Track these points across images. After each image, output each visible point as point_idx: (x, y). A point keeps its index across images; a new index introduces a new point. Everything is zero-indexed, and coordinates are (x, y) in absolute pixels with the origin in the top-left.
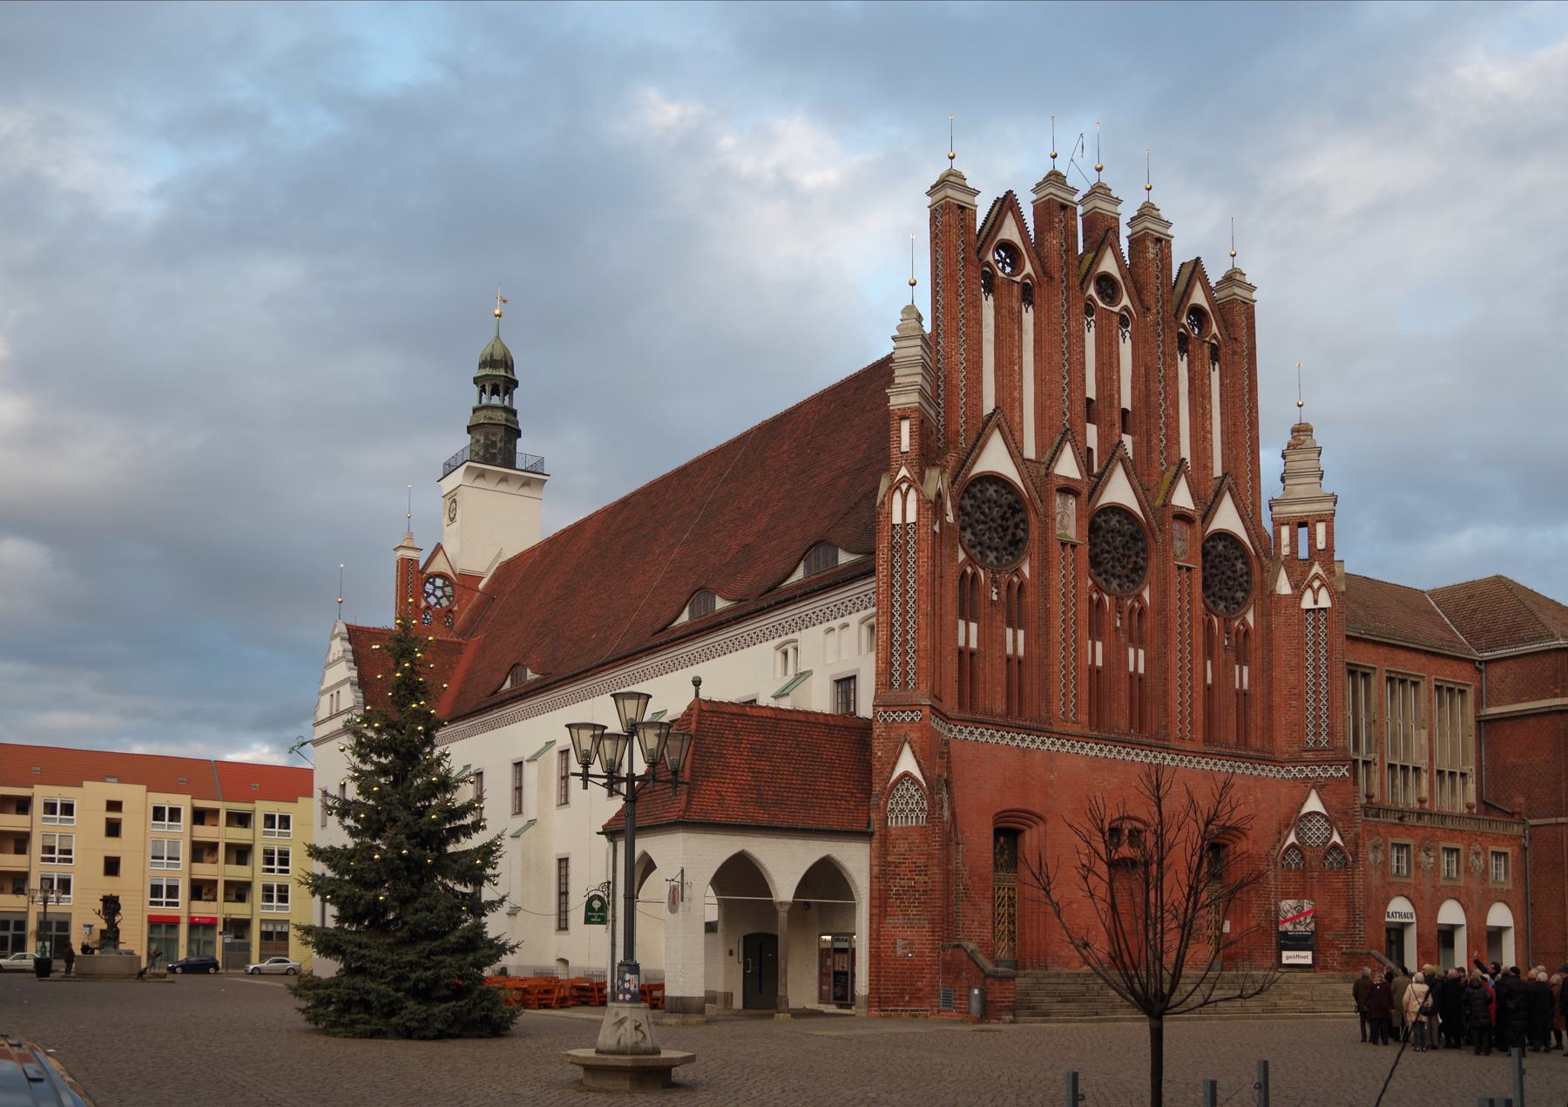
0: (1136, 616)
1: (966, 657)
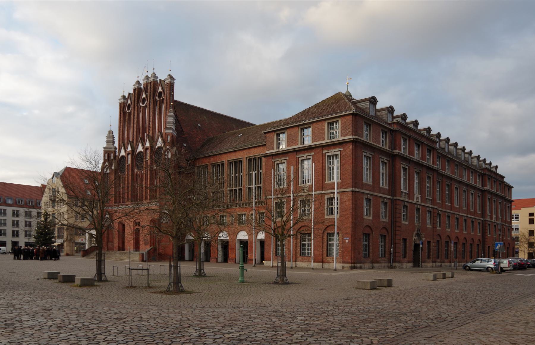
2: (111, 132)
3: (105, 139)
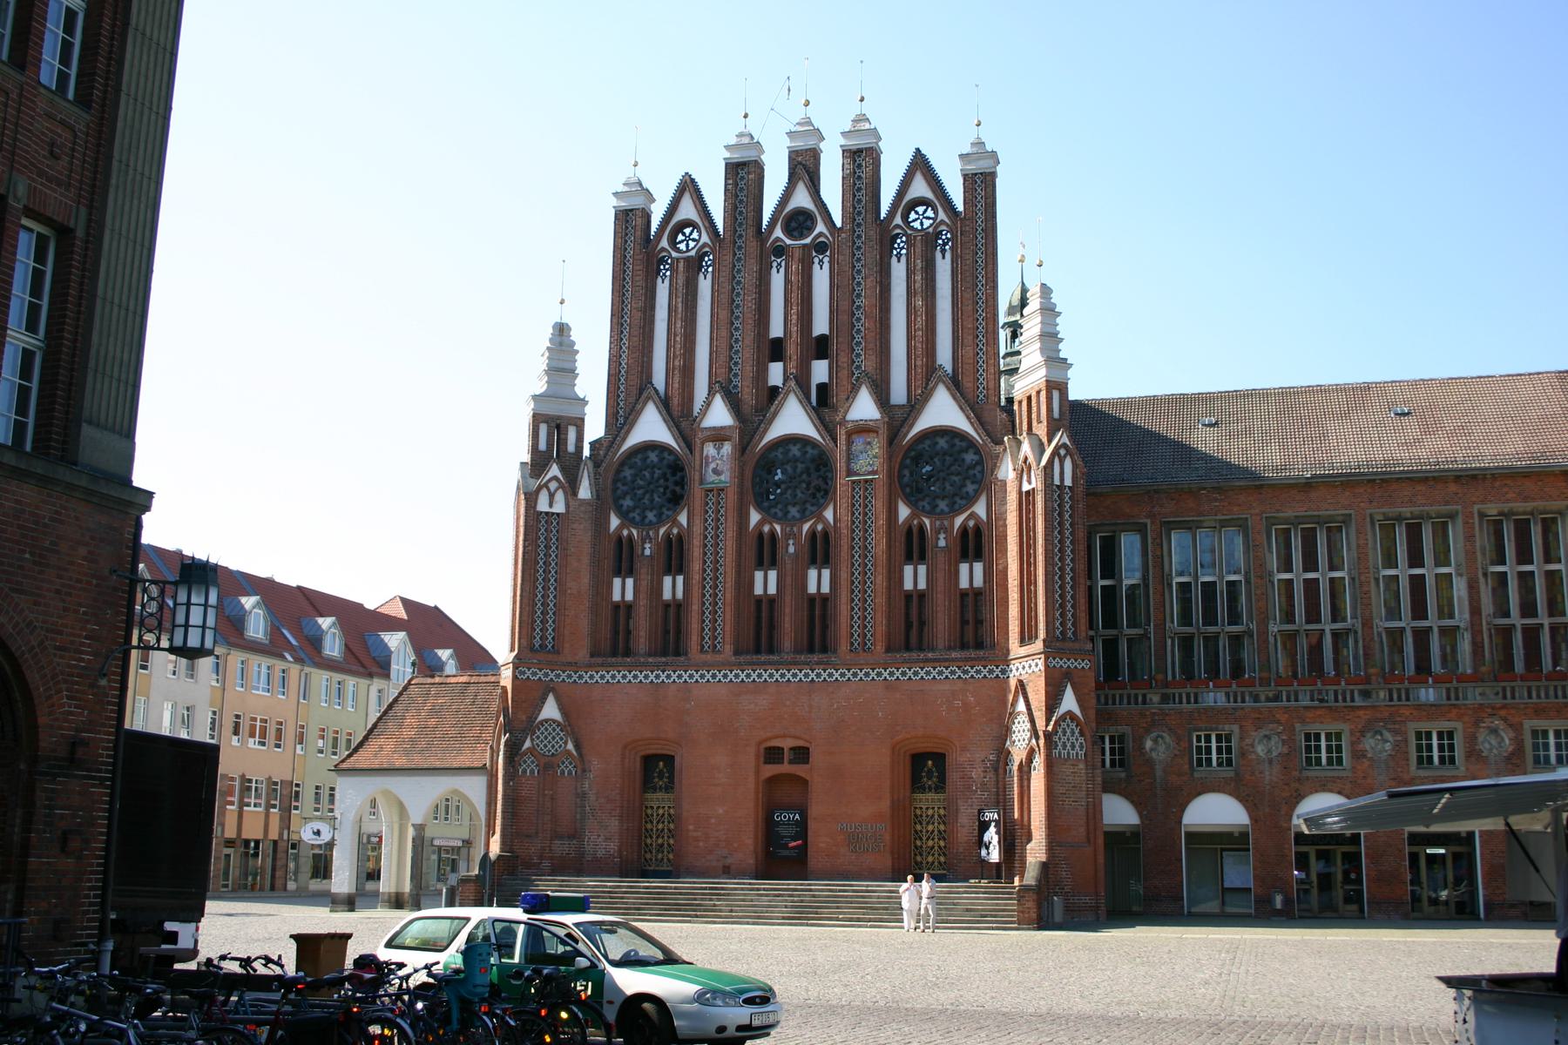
1: (624, 611)
2: (561, 330)
3: (542, 364)
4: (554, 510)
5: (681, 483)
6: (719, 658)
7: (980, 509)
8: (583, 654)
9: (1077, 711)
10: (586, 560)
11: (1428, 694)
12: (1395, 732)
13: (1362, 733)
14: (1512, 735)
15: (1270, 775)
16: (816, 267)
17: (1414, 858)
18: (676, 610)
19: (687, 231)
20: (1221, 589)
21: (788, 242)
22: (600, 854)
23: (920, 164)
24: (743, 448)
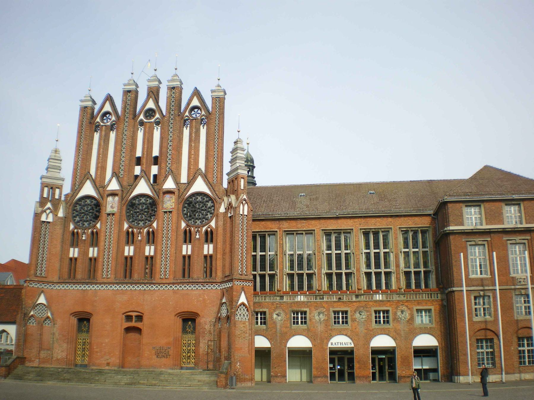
0: (151, 235)
4: (48, 221)
5: (99, 211)
6: (109, 281)
7: (213, 224)
8: (56, 279)
9: (246, 302)
10: (59, 240)
11: (379, 297)
12: (367, 311)
13: (355, 312)
14: (409, 312)
15: (320, 328)
16: (155, 130)
17: (373, 360)
18: (93, 261)
19: (107, 116)
20: (305, 256)
21: (145, 120)
22: (59, 357)
23: (197, 93)
24: (122, 199)
